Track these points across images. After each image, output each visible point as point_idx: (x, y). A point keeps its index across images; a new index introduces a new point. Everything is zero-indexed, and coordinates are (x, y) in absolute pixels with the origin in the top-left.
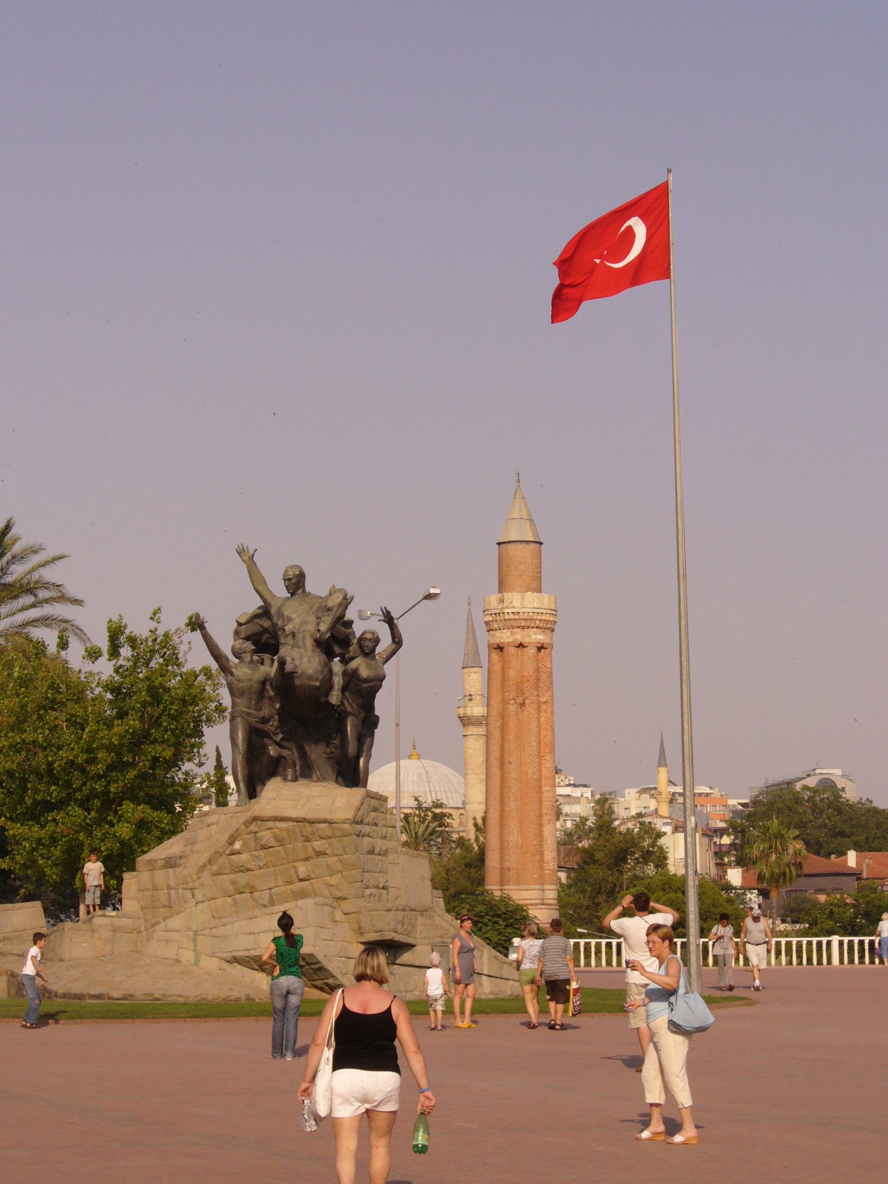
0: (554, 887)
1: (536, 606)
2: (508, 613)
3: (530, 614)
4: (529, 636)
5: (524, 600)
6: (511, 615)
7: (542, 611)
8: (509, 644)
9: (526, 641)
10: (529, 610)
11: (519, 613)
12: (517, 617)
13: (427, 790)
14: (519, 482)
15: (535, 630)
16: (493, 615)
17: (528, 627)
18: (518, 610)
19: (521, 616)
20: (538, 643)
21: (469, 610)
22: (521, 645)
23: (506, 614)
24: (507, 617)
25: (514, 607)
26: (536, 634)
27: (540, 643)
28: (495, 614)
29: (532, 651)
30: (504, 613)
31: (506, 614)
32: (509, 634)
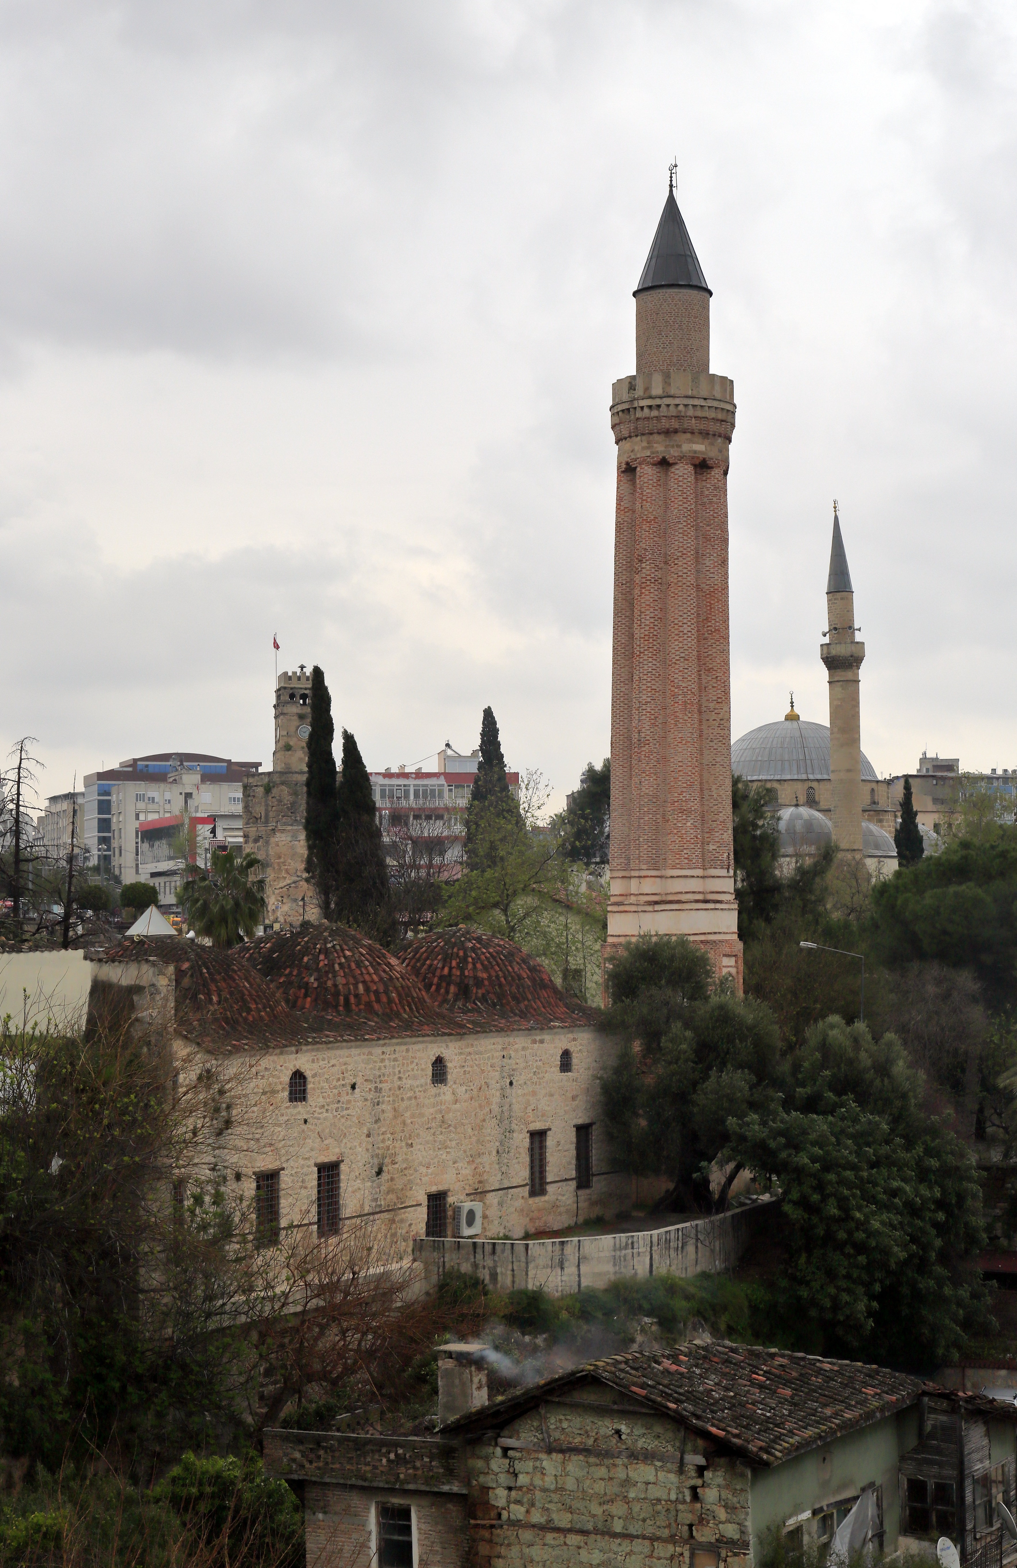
0: (723, 872)
1: (690, 393)
2: (642, 408)
3: (681, 408)
4: (679, 446)
5: (670, 384)
6: (646, 410)
7: (701, 402)
8: (643, 461)
9: (672, 453)
10: (677, 401)
11: (659, 406)
12: (655, 413)
13: (801, 757)
14: (671, 186)
15: (688, 435)
16: (620, 413)
17: (676, 431)
18: (658, 402)
19: (664, 411)
20: (693, 458)
21: (836, 518)
22: (664, 464)
23: (638, 410)
24: (639, 414)
25: (650, 397)
26: (691, 441)
27: (698, 458)
28: (623, 411)
29: (683, 471)
30: (635, 408)
31: (638, 410)
32: (645, 444)
